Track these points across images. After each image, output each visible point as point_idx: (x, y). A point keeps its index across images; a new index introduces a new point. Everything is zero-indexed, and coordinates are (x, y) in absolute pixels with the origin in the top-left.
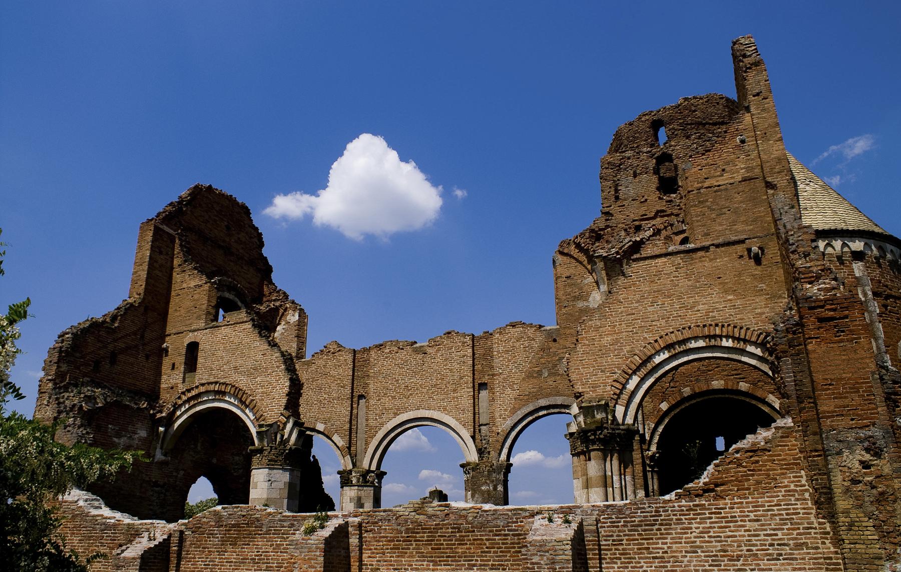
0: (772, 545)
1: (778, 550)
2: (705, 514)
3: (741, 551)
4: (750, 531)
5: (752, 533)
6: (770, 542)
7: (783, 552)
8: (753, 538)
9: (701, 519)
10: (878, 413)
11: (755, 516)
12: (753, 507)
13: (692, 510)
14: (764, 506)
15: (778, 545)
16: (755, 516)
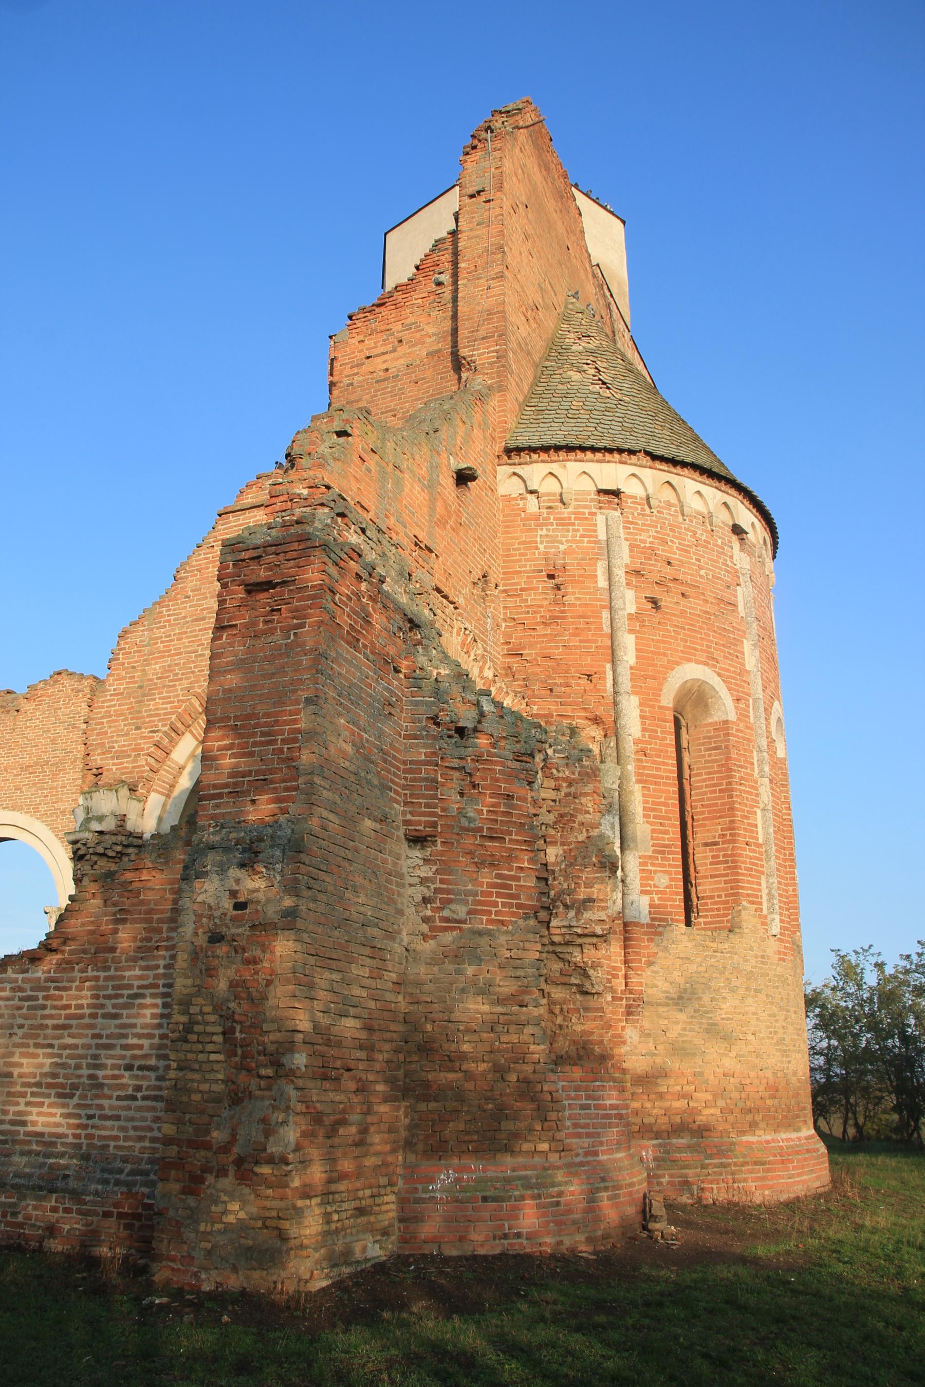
0: (129, 1068)
1: (137, 1077)
2: (37, 998)
3: (80, 1076)
4: (99, 1036)
5: (104, 1041)
6: (127, 1061)
7: (145, 1084)
8: (103, 1052)
9: (29, 1008)
10: (296, 788)
11: (114, 1006)
12: (114, 988)
13: (21, 989)
14: (130, 987)
15: (141, 1068)
16: (114, 1006)
